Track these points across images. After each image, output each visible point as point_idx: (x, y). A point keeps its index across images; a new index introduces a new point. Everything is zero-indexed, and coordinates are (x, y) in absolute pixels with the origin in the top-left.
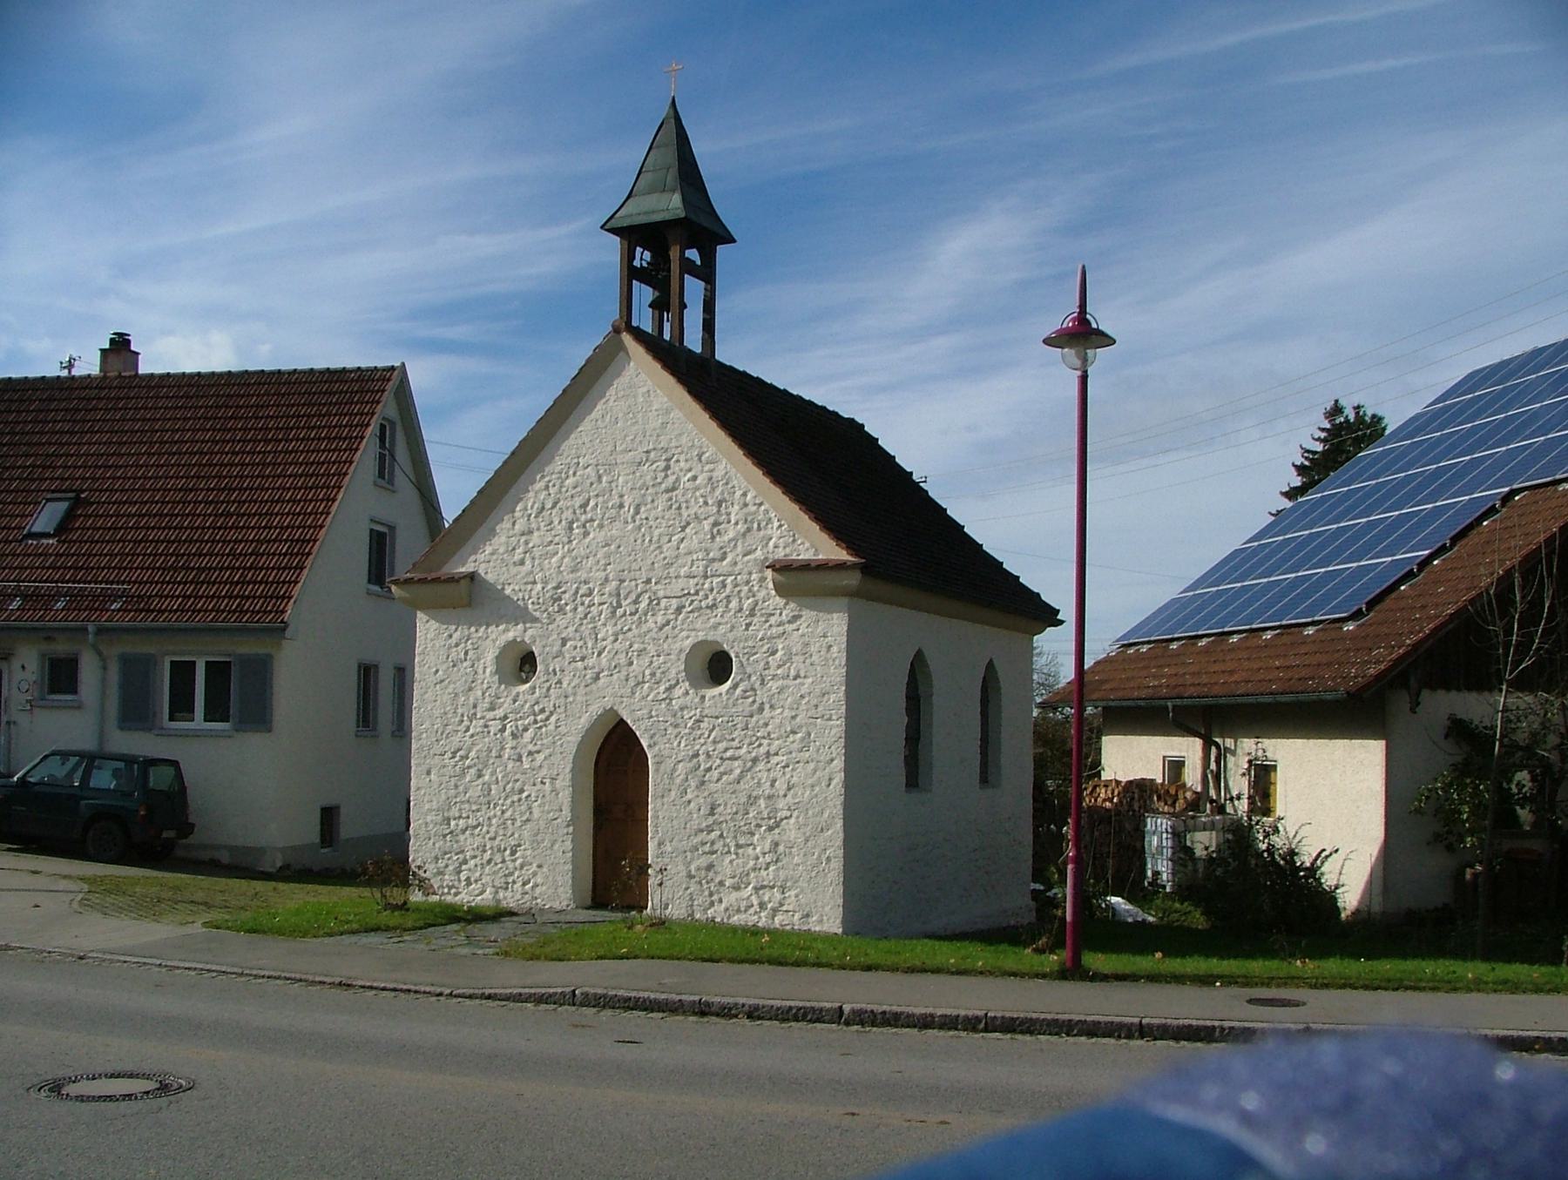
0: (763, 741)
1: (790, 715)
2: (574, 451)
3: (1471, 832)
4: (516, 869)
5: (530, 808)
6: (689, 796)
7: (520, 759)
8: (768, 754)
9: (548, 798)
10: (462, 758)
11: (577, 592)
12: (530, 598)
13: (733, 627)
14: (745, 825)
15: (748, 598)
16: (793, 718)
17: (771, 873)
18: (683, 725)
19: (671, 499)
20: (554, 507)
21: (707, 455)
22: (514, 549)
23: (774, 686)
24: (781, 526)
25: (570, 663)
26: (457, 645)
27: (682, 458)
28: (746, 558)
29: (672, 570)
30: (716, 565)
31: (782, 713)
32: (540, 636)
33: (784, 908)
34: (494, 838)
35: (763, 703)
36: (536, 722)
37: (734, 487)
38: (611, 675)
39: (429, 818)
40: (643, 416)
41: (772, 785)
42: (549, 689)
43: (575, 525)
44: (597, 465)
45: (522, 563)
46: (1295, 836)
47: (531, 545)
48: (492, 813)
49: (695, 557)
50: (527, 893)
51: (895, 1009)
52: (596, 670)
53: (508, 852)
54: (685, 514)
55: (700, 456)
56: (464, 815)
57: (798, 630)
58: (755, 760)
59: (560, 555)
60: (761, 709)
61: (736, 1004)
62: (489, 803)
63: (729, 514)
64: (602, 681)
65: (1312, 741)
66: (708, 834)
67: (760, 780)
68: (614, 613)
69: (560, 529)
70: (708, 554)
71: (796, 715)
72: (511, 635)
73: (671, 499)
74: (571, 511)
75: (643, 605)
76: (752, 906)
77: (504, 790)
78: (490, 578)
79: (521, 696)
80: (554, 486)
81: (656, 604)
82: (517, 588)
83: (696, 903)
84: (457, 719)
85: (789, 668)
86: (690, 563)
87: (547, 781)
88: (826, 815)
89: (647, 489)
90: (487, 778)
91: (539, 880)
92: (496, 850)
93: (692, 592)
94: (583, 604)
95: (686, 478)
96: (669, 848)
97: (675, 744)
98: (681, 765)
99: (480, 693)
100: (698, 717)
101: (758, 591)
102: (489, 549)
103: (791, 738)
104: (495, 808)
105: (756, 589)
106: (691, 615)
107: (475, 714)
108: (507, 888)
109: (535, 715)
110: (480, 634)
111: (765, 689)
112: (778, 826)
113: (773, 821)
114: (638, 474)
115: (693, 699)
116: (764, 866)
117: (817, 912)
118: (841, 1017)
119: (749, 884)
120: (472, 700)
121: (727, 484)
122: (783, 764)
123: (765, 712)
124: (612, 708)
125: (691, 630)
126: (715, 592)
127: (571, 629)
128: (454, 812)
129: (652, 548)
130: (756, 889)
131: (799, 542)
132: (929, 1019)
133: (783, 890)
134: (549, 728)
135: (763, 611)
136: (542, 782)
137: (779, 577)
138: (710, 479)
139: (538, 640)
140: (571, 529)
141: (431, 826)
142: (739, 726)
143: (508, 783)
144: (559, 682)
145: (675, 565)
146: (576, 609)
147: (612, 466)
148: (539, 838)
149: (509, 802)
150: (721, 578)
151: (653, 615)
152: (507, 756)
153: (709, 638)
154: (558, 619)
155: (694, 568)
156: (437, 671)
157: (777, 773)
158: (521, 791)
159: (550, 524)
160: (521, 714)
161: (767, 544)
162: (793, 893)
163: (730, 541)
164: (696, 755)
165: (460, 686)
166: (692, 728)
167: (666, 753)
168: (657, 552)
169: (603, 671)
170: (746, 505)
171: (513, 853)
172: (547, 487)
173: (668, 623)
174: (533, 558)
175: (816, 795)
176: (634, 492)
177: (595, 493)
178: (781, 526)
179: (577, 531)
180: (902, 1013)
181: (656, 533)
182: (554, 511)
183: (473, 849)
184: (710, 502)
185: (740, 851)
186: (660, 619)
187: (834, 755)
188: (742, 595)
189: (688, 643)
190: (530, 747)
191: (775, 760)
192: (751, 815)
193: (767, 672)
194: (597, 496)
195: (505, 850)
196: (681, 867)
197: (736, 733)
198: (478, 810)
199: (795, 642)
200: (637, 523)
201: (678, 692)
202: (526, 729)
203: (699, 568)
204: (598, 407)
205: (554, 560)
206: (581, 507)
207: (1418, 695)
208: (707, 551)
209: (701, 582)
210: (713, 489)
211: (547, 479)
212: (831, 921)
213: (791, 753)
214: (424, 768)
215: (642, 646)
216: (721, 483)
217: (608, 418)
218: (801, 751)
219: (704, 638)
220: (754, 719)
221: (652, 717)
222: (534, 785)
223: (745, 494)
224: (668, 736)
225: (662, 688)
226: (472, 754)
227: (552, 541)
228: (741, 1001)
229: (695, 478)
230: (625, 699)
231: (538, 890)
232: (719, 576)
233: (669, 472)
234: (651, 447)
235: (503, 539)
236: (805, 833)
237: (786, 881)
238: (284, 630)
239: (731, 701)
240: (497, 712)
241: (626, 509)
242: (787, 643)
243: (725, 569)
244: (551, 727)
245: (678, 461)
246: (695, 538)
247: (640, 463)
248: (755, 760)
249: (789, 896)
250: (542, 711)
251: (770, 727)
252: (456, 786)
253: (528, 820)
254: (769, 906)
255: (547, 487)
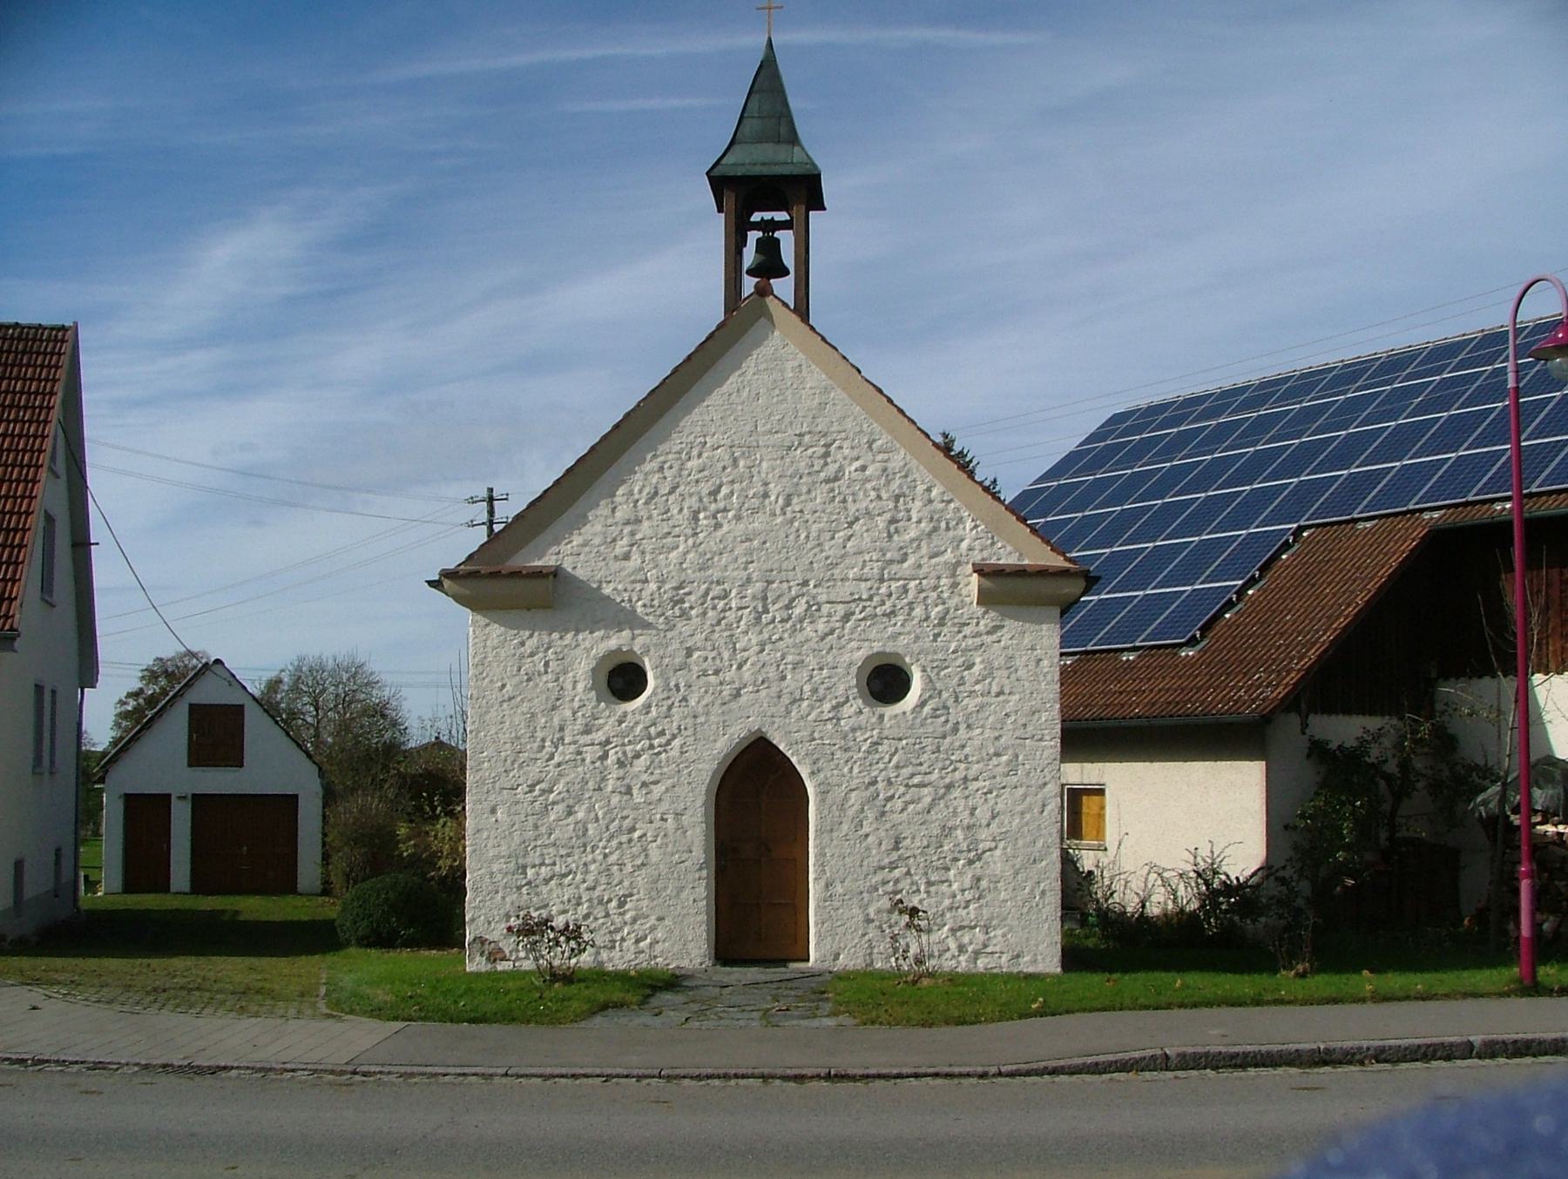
0: (958, 765)
1: (992, 736)
2: (699, 429)
3: (1347, 848)
4: (625, 923)
5: (645, 850)
6: (866, 829)
7: (629, 791)
8: (965, 779)
9: (671, 838)
10: (543, 791)
11: (707, 593)
12: (639, 599)
13: (917, 638)
14: (938, 860)
15: (936, 606)
16: (997, 738)
17: (972, 912)
18: (856, 748)
19: (832, 490)
20: (673, 490)
21: (880, 442)
22: (614, 540)
23: (971, 704)
24: (976, 527)
25: (698, 677)
26: (532, 655)
27: (846, 444)
28: (934, 561)
29: (836, 571)
30: (895, 568)
31: (982, 733)
32: (656, 645)
33: (989, 950)
34: (594, 888)
35: (958, 723)
36: (652, 747)
37: (914, 481)
38: (758, 691)
39: (495, 867)
40: (794, 394)
41: (972, 814)
42: (670, 708)
43: (701, 516)
44: (731, 447)
45: (627, 557)
46: (1218, 856)
47: (638, 537)
48: (590, 857)
49: (867, 558)
50: (643, 952)
51: (1530, 1036)
52: (737, 685)
53: (614, 904)
54: (852, 508)
55: (870, 444)
56: (547, 862)
57: (999, 641)
58: (949, 787)
59: (681, 549)
60: (955, 730)
61: (1360, 1048)
62: (585, 846)
63: (908, 511)
64: (743, 699)
65: (1157, 765)
66: (890, 872)
67: (955, 808)
68: (758, 619)
69: (681, 519)
70: (884, 555)
71: (1000, 736)
72: (613, 643)
73: (832, 490)
74: (695, 498)
75: (798, 610)
76: (948, 949)
77: (608, 829)
78: (581, 573)
79: (629, 716)
80: (671, 467)
81: (816, 610)
82: (620, 587)
83: (875, 951)
84: (536, 745)
85: (990, 684)
86: (861, 564)
87: (670, 818)
88: (1040, 844)
89: (801, 477)
90: (580, 815)
91: (659, 935)
92: (596, 902)
93: (864, 597)
94: (714, 608)
95: (853, 468)
96: (839, 889)
97: (846, 770)
98: (853, 794)
99: (568, 713)
100: (875, 739)
101: (950, 598)
102: (577, 540)
103: (995, 761)
104: (593, 852)
105: (945, 595)
106: (863, 623)
107: (562, 739)
108: (614, 947)
109: (650, 738)
110: (566, 642)
111: (959, 708)
112: (979, 859)
113: (973, 854)
114: (788, 460)
115: (869, 717)
116: (963, 905)
117: (1029, 952)
118: (1472, 1050)
119: (945, 925)
120: (556, 721)
121: (906, 476)
122: (985, 790)
123: (961, 732)
124: (759, 729)
125: (864, 640)
126: (894, 596)
127: (699, 637)
128: (534, 858)
129: (809, 546)
130: (953, 931)
131: (999, 545)
132: (1561, 1044)
133: (986, 929)
134: (671, 754)
135: (956, 621)
136: (662, 819)
137: (987, 583)
138: (885, 470)
139: (652, 649)
140: (696, 519)
141: (499, 877)
142: (929, 748)
143: (613, 820)
144: (685, 699)
145: (842, 565)
146: (704, 613)
147: (750, 449)
148: (660, 885)
149: (614, 843)
150: (901, 582)
151: (811, 622)
152: (610, 788)
153: (888, 650)
154: (679, 625)
155: (865, 571)
156: (504, 686)
157: (977, 800)
158: (632, 830)
159: (666, 513)
160: (630, 738)
161: (958, 546)
162: (999, 932)
163: (913, 540)
164: (874, 782)
165: (539, 704)
166: (868, 752)
167: (834, 780)
168: (817, 550)
169: (745, 686)
170: (930, 501)
171: (621, 904)
172: (661, 469)
173: (832, 632)
174: (643, 553)
175: (1027, 824)
176: (784, 480)
177: (730, 478)
178: (976, 527)
179: (705, 522)
180: (1533, 1041)
181: (815, 527)
182: (672, 498)
183: (562, 902)
184: (884, 496)
185: (933, 889)
186: (821, 626)
187: (1047, 779)
188: (929, 601)
189: (860, 656)
190: (645, 777)
191: (973, 786)
192: (946, 848)
193: (962, 688)
194: (733, 482)
195: (610, 900)
196: (856, 911)
197: (925, 756)
198: (568, 855)
199: (996, 654)
200: (789, 515)
201: (847, 710)
202: (637, 756)
203: (873, 570)
204: (731, 379)
205: (673, 555)
206: (710, 494)
207: (1307, 717)
208: (883, 551)
209: (876, 586)
210: (888, 482)
211: (661, 459)
212: (1048, 960)
213: (994, 777)
214: (487, 806)
215: (798, 658)
216: (898, 475)
217: (745, 394)
218: (1008, 775)
219: (881, 649)
220: (948, 740)
221: (814, 739)
222: (651, 822)
223: (929, 490)
224: (836, 762)
225: (827, 706)
226: (560, 787)
227: (669, 533)
228: (1365, 1044)
229: (864, 468)
230: (777, 720)
231: (658, 948)
232: (899, 579)
233: (829, 460)
234: (805, 429)
235: (598, 528)
236: (1014, 866)
237: (991, 919)
238: (13, 639)
239: (919, 720)
240: (593, 736)
241: (773, 498)
242: (986, 656)
243: (908, 572)
244: (674, 753)
245: (840, 448)
246: (865, 535)
247: (790, 448)
248: (949, 787)
249: (995, 936)
250: (662, 733)
251: (967, 750)
252: (536, 827)
253: (643, 864)
254: (970, 949)
255: (661, 469)
